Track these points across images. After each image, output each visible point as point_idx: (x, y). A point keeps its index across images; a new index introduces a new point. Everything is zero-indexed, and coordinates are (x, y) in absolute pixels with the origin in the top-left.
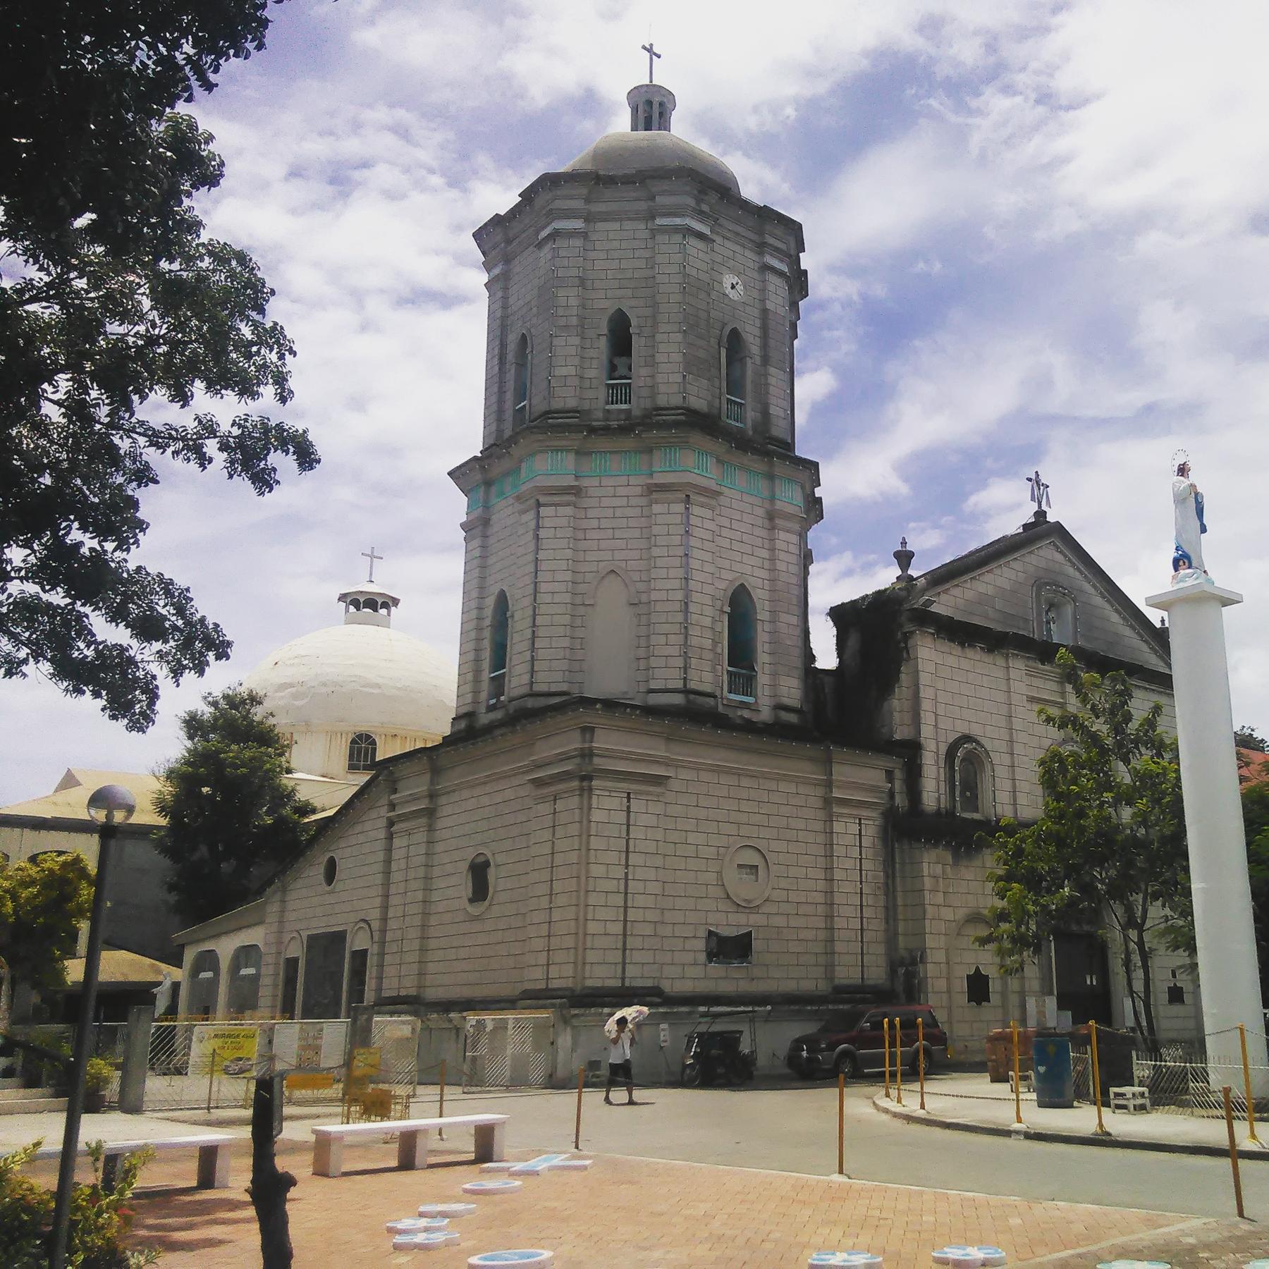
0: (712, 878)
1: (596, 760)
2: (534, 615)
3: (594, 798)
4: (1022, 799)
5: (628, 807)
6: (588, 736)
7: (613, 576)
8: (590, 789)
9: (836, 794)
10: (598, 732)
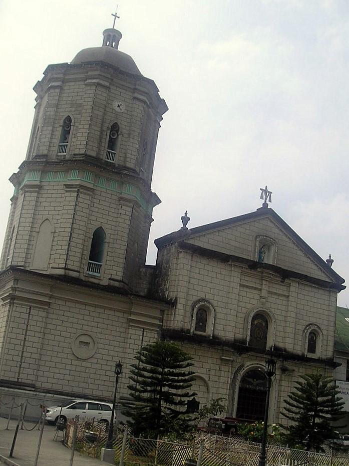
5: (30, 312)
7: (47, 221)
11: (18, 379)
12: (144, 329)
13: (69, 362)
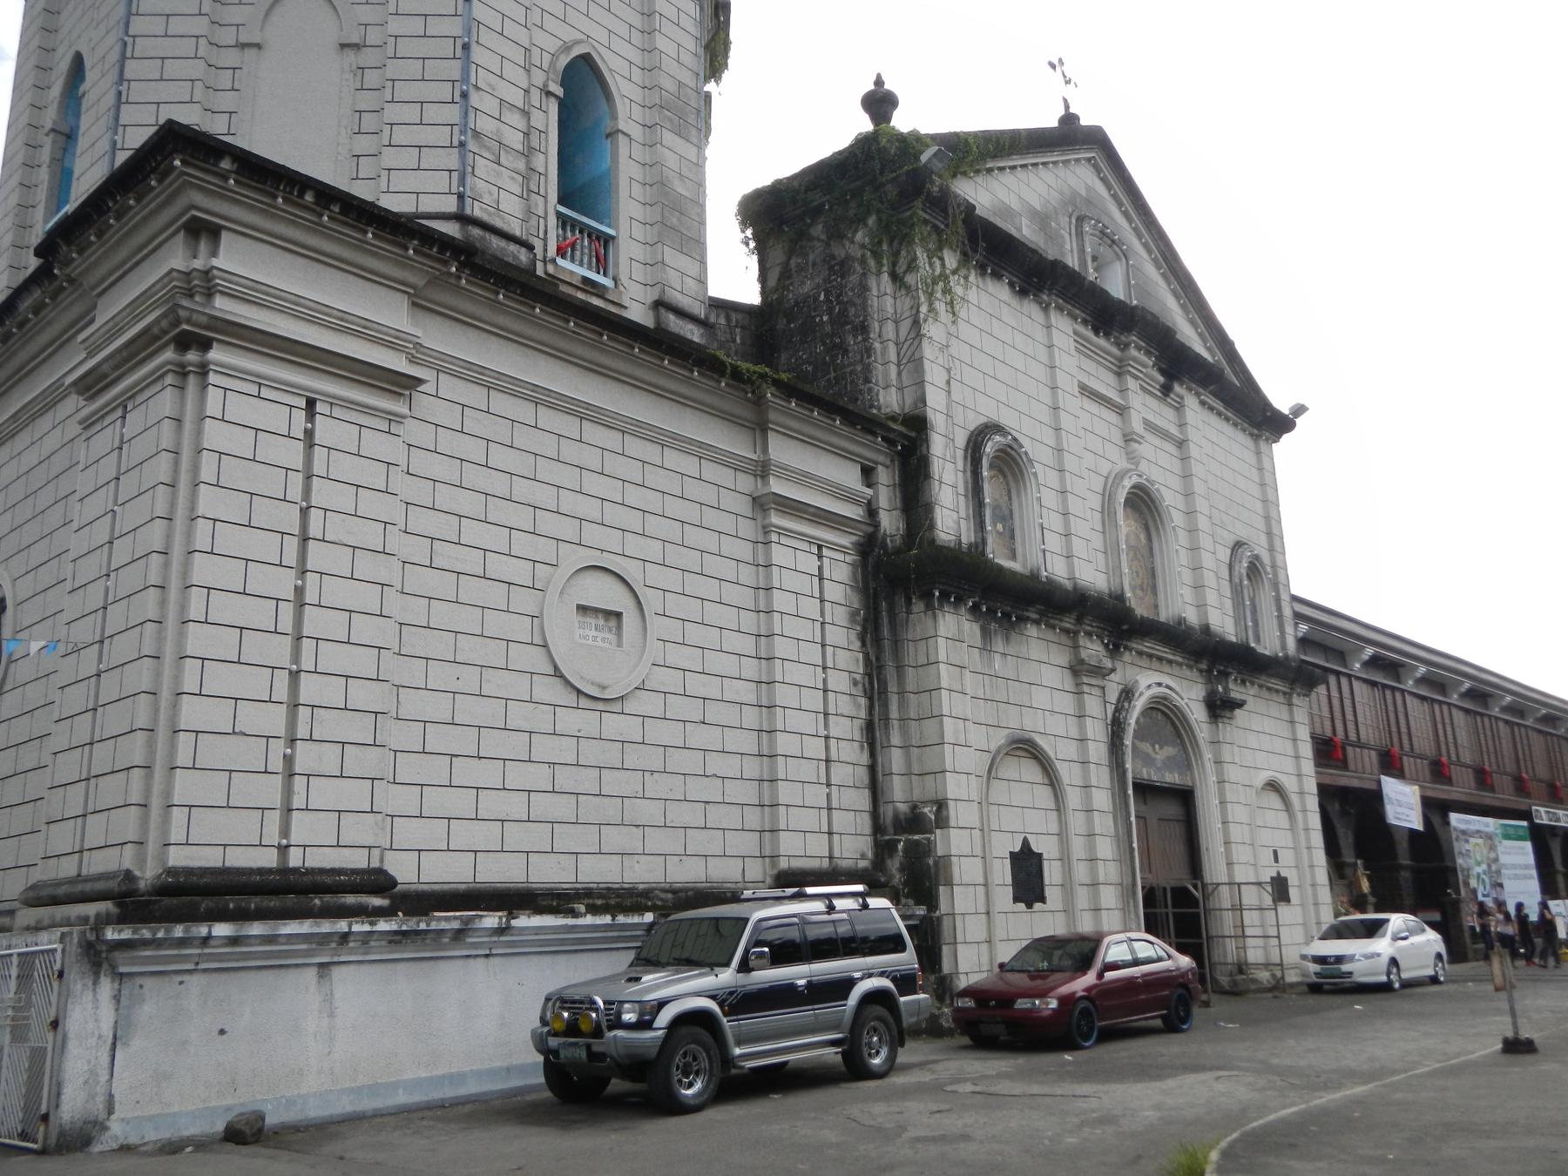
0: (520, 628)
1: (220, 302)
2: (123, 58)
3: (214, 395)
4: (1078, 547)
5: (309, 434)
6: (203, 246)
8: (203, 370)
9: (777, 486)
10: (225, 237)
11: (283, 850)
12: (820, 547)
13: (541, 719)
